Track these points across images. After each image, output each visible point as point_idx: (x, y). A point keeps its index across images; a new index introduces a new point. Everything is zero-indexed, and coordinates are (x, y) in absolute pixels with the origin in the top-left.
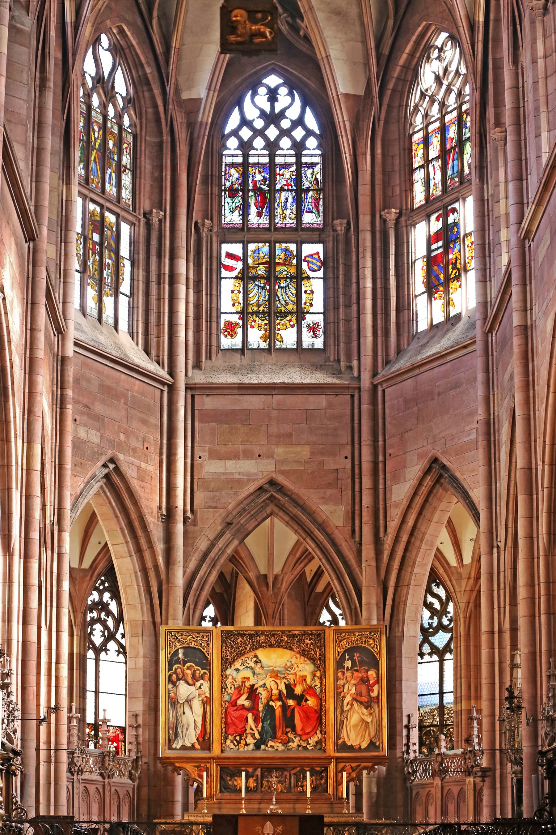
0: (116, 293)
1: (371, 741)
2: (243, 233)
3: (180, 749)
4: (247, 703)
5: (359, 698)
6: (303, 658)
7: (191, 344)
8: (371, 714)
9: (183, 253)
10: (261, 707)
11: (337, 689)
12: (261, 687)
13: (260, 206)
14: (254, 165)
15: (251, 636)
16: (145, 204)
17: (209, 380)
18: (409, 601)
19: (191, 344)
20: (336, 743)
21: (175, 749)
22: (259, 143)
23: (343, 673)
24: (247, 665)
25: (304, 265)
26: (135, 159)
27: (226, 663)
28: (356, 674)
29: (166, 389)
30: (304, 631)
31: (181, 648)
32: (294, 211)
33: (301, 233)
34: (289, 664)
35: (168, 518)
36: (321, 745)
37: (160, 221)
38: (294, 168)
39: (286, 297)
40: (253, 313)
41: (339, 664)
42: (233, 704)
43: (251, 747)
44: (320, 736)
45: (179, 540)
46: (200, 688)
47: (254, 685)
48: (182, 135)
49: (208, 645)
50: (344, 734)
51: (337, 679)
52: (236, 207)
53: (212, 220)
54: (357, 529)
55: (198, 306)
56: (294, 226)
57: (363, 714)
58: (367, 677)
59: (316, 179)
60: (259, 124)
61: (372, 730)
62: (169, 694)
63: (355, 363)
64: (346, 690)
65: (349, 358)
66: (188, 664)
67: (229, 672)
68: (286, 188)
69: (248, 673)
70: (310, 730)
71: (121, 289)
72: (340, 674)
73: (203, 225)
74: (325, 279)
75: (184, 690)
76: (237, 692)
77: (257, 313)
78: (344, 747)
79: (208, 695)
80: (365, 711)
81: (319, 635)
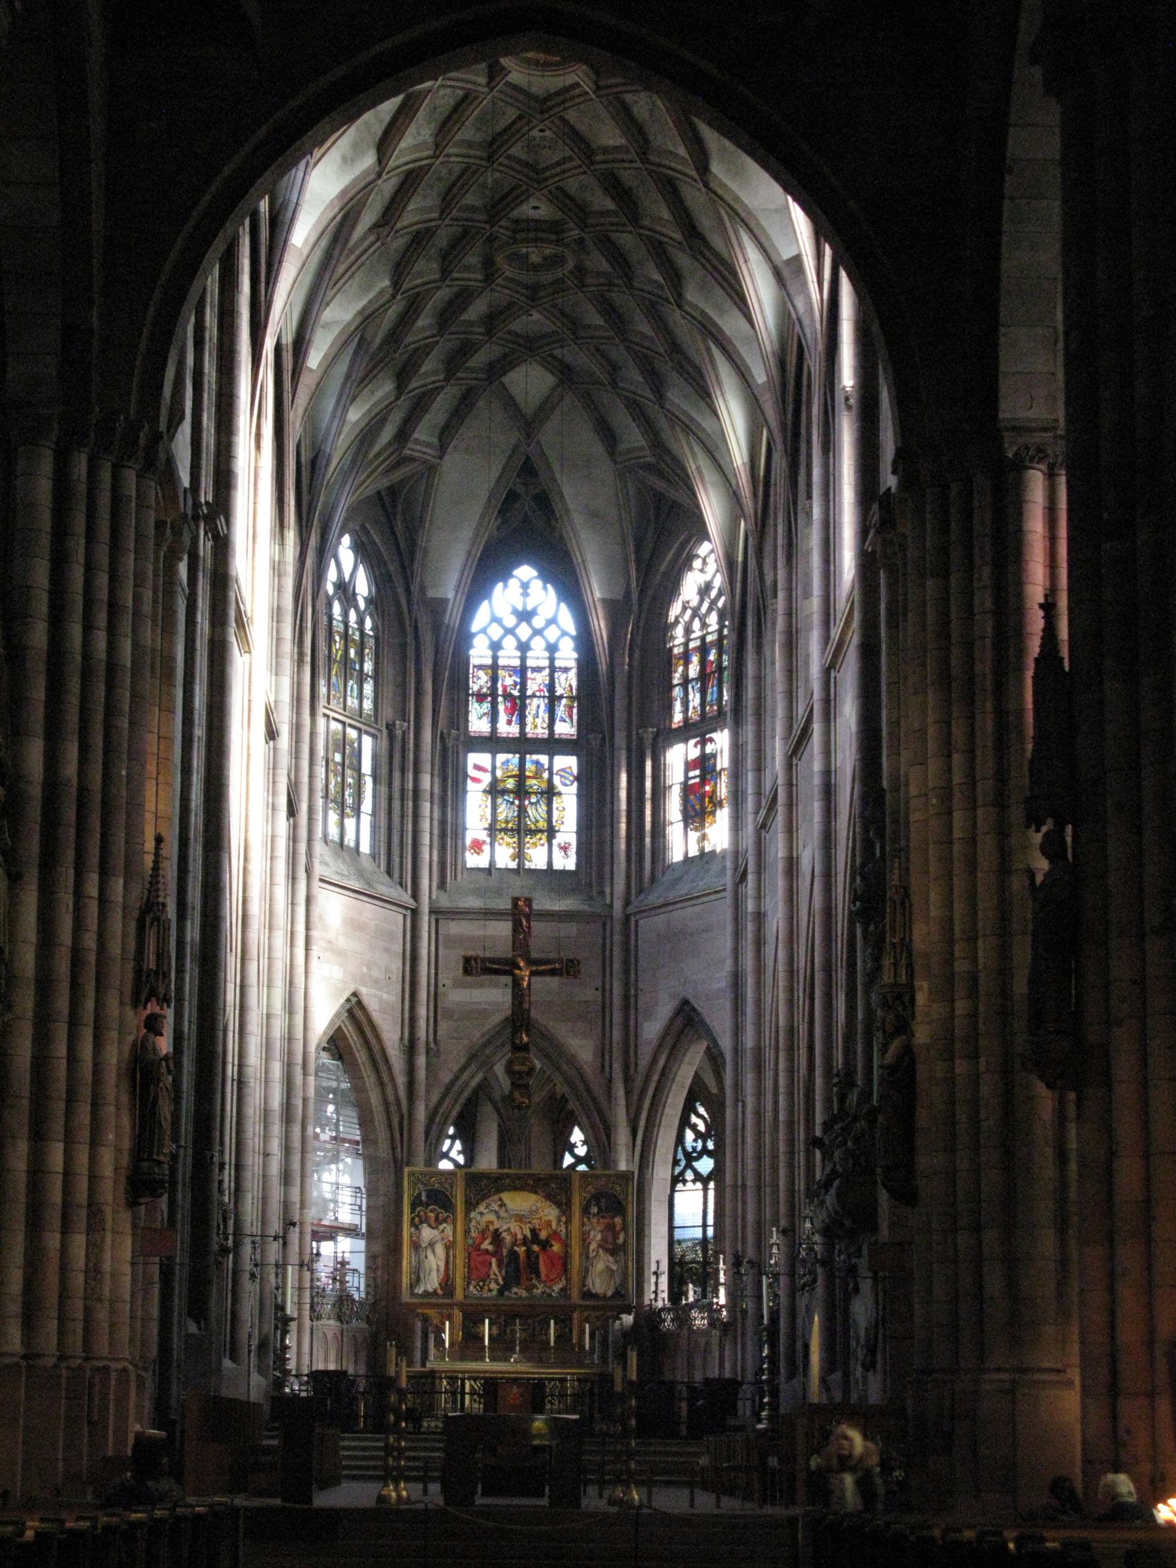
0: (357, 811)
2: (493, 743)
4: (490, 1248)
7: (435, 864)
9: (427, 767)
13: (510, 712)
14: (504, 667)
16: (388, 713)
17: (454, 904)
18: (659, 1143)
19: (435, 864)
20: (581, 1291)
22: (509, 643)
25: (556, 780)
26: (377, 664)
27: (470, 1205)
28: (602, 1221)
29: (409, 913)
32: (547, 720)
33: (553, 745)
35: (410, 1049)
37: (404, 732)
38: (547, 671)
39: (536, 813)
40: (501, 830)
41: (586, 1211)
43: (494, 1293)
45: (421, 1074)
47: (497, 1230)
48: (427, 638)
50: (589, 1281)
51: (583, 1225)
52: (485, 714)
53: (458, 729)
54: (607, 1064)
55: (443, 823)
56: (546, 736)
59: (570, 686)
60: (510, 621)
63: (608, 890)
65: (601, 883)
67: (472, 1215)
68: (538, 694)
69: (492, 1217)
71: (363, 808)
73: (449, 735)
74: (579, 796)
75: (427, 1233)
77: (505, 830)
78: (588, 1295)
80: (610, 1258)
81: (565, 1180)
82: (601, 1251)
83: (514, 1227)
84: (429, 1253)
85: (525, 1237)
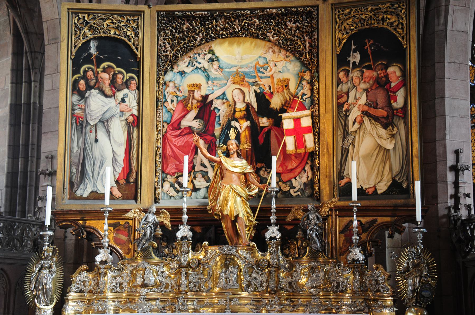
1: (394, 180)
3: (87, 198)
4: (196, 125)
5: (372, 111)
6: (283, 52)
8: (393, 136)
10: (217, 130)
11: (338, 99)
12: (218, 98)
15: (203, 19)
21: (81, 198)
23: (347, 73)
24: (197, 65)
28: (367, 73)
30: (286, 8)
31: (94, 39)
34: (261, 62)
36: (313, 189)
41: (342, 60)
42: (176, 125)
44: (310, 175)
46: (123, 100)
47: (207, 96)
49: (136, 34)
57: (380, 137)
58: (386, 76)
61: (396, 162)
62: (73, 110)
64: (351, 100)
66: (105, 64)
67: (169, 77)
69: (198, 78)
70: (295, 165)
72: (341, 74)
75: (97, 104)
76: (181, 106)
79: (135, 113)
80: (382, 132)
81: (309, 14)
82: (366, 120)
83: (232, 92)
84: (102, 135)
85: (248, 106)
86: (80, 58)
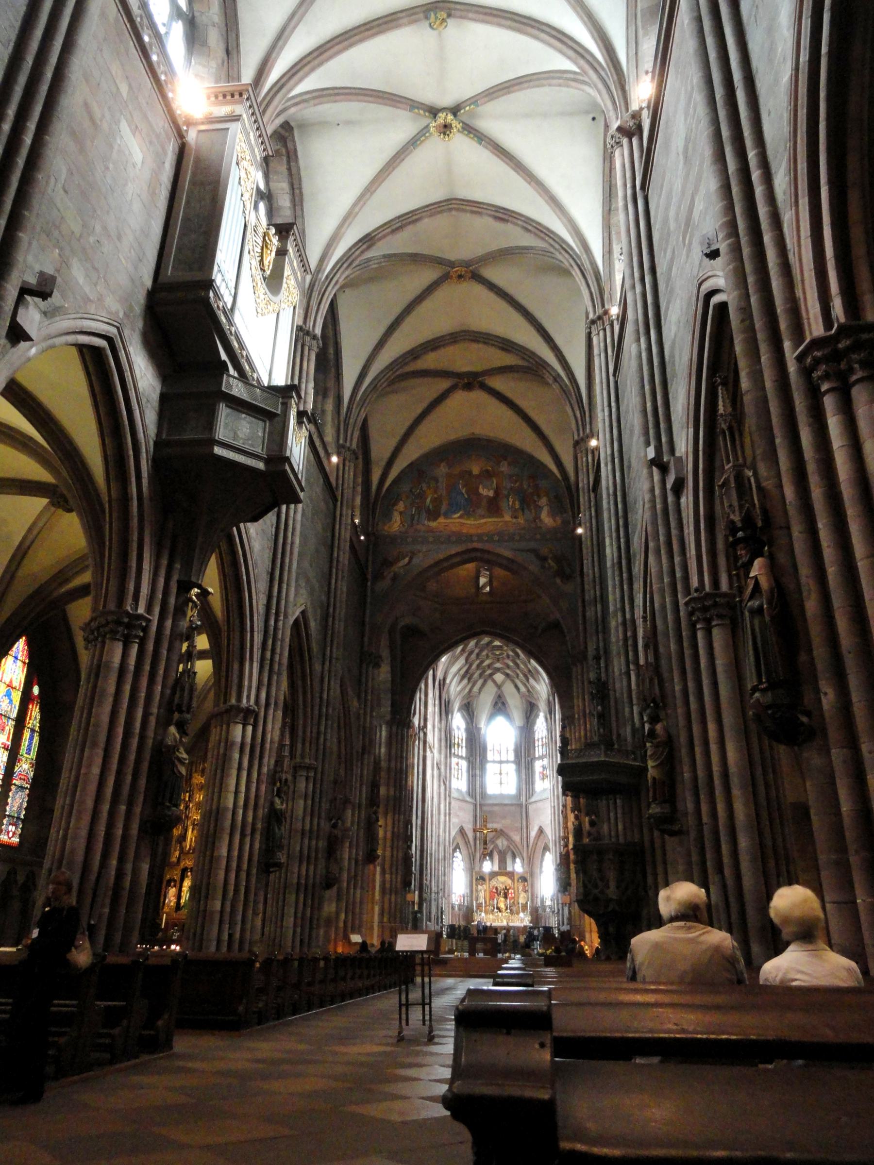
2: (494, 762)
33: (507, 762)
41: (518, 881)
75: (480, 887)
86: (477, 879)
